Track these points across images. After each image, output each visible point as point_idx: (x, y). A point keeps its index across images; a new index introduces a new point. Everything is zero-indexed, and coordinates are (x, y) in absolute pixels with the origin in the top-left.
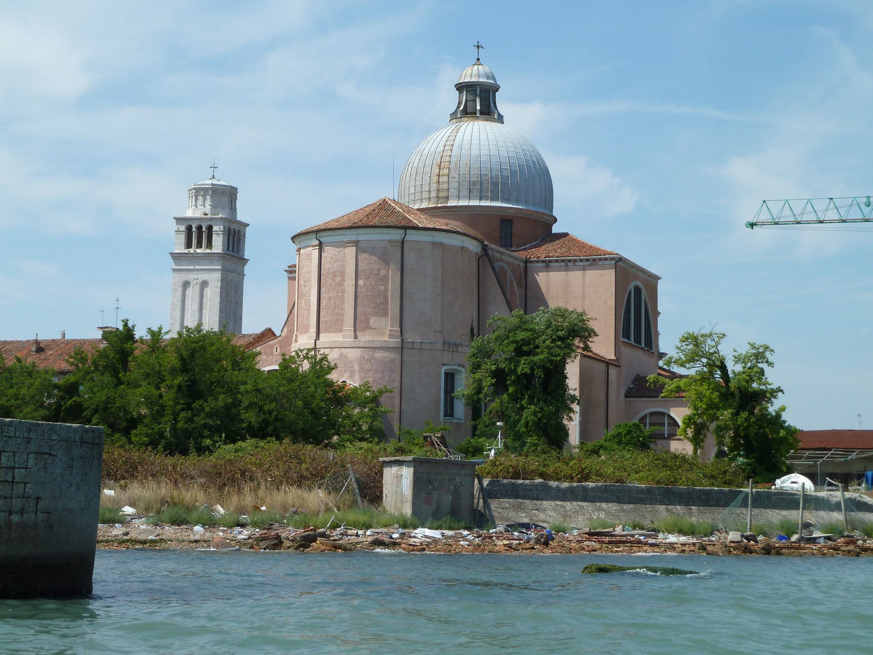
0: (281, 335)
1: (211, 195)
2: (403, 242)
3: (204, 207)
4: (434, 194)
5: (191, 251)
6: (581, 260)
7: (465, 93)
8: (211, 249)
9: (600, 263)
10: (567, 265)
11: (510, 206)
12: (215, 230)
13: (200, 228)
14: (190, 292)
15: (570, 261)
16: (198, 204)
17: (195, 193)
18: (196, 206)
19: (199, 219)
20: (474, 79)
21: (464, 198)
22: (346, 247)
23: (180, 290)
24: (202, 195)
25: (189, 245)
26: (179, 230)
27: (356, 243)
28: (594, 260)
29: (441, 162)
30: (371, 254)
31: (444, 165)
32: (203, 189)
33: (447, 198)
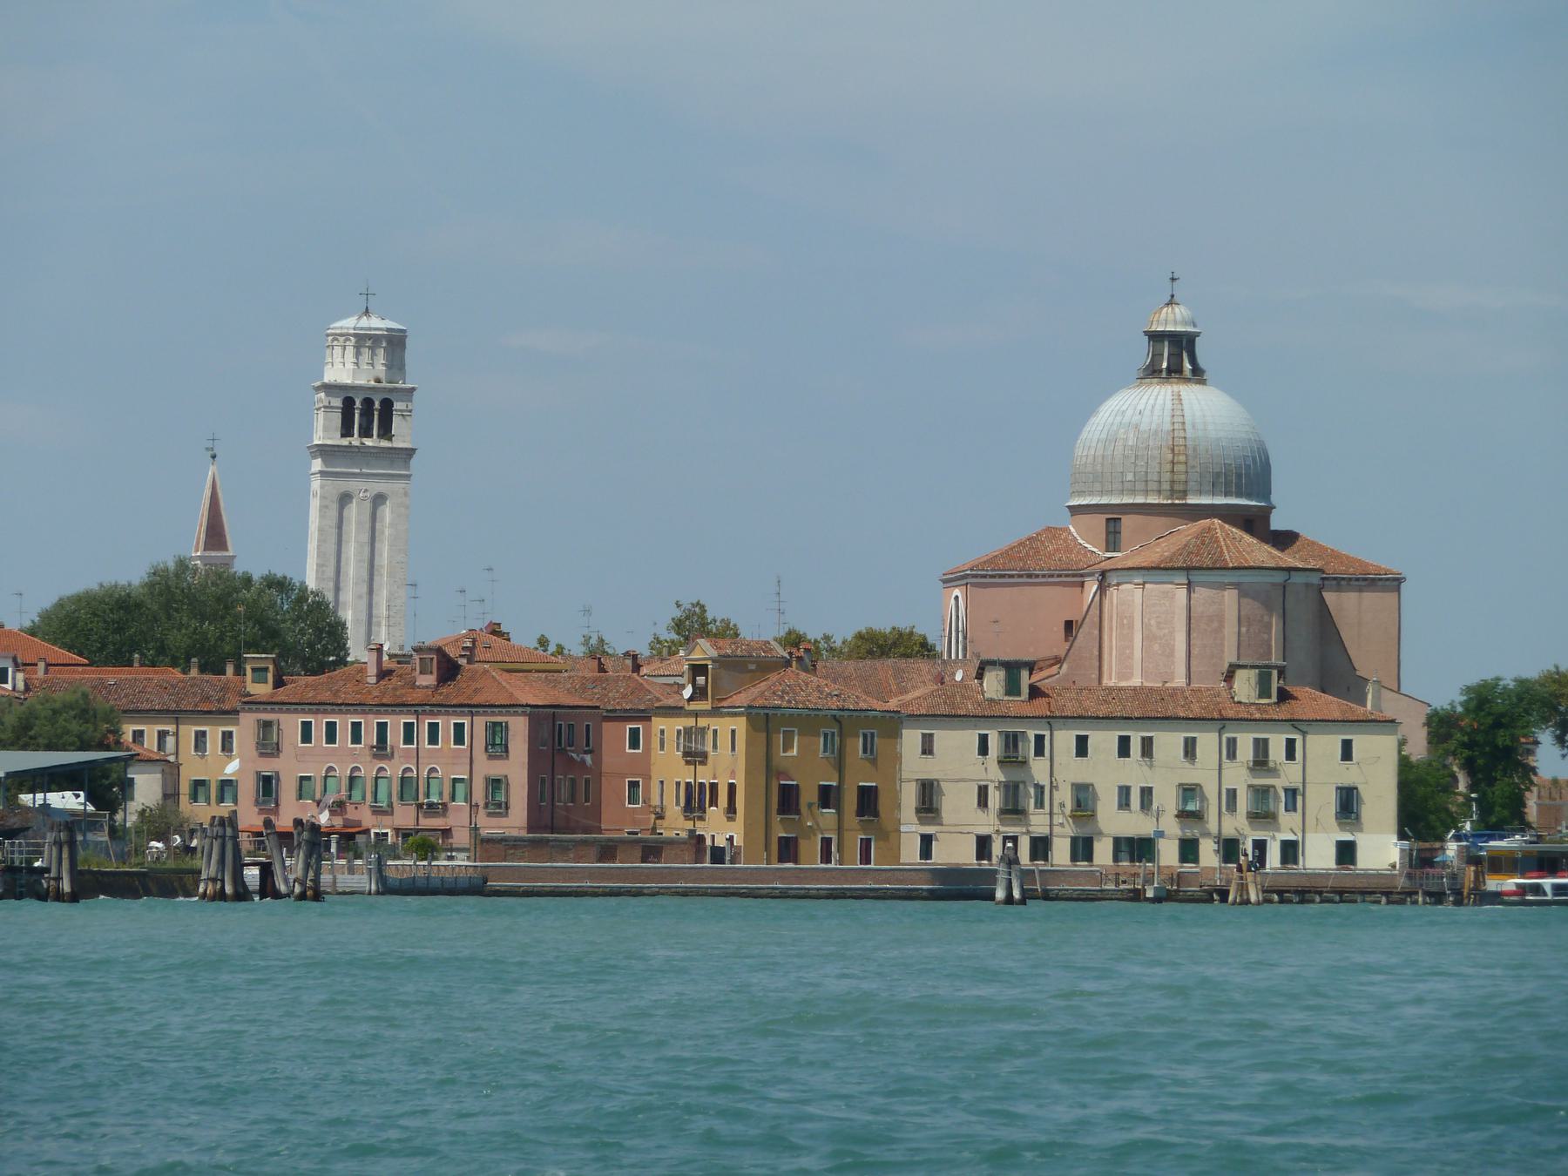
0: (1059, 673)
1: (385, 348)
2: (1284, 587)
3: (374, 368)
4: (1166, 486)
5: (355, 441)
6: (1357, 579)
7: (1166, 343)
8: (390, 439)
9: (1380, 583)
10: (1339, 584)
11: (1253, 503)
12: (398, 408)
13: (368, 403)
14: (352, 511)
15: (1343, 579)
16: (360, 362)
17: (356, 342)
18: (357, 364)
19: (370, 388)
20: (1179, 329)
21: (1207, 493)
22: (1225, 589)
23: (335, 506)
24: (369, 348)
25: (347, 431)
26: (332, 404)
27: (1237, 586)
28: (1373, 579)
29: (1173, 445)
30: (1254, 598)
31: (1179, 451)
32: (370, 337)
33: (1184, 493)
